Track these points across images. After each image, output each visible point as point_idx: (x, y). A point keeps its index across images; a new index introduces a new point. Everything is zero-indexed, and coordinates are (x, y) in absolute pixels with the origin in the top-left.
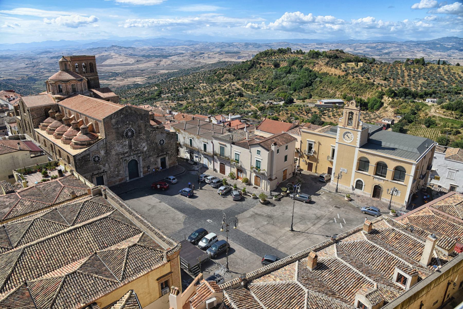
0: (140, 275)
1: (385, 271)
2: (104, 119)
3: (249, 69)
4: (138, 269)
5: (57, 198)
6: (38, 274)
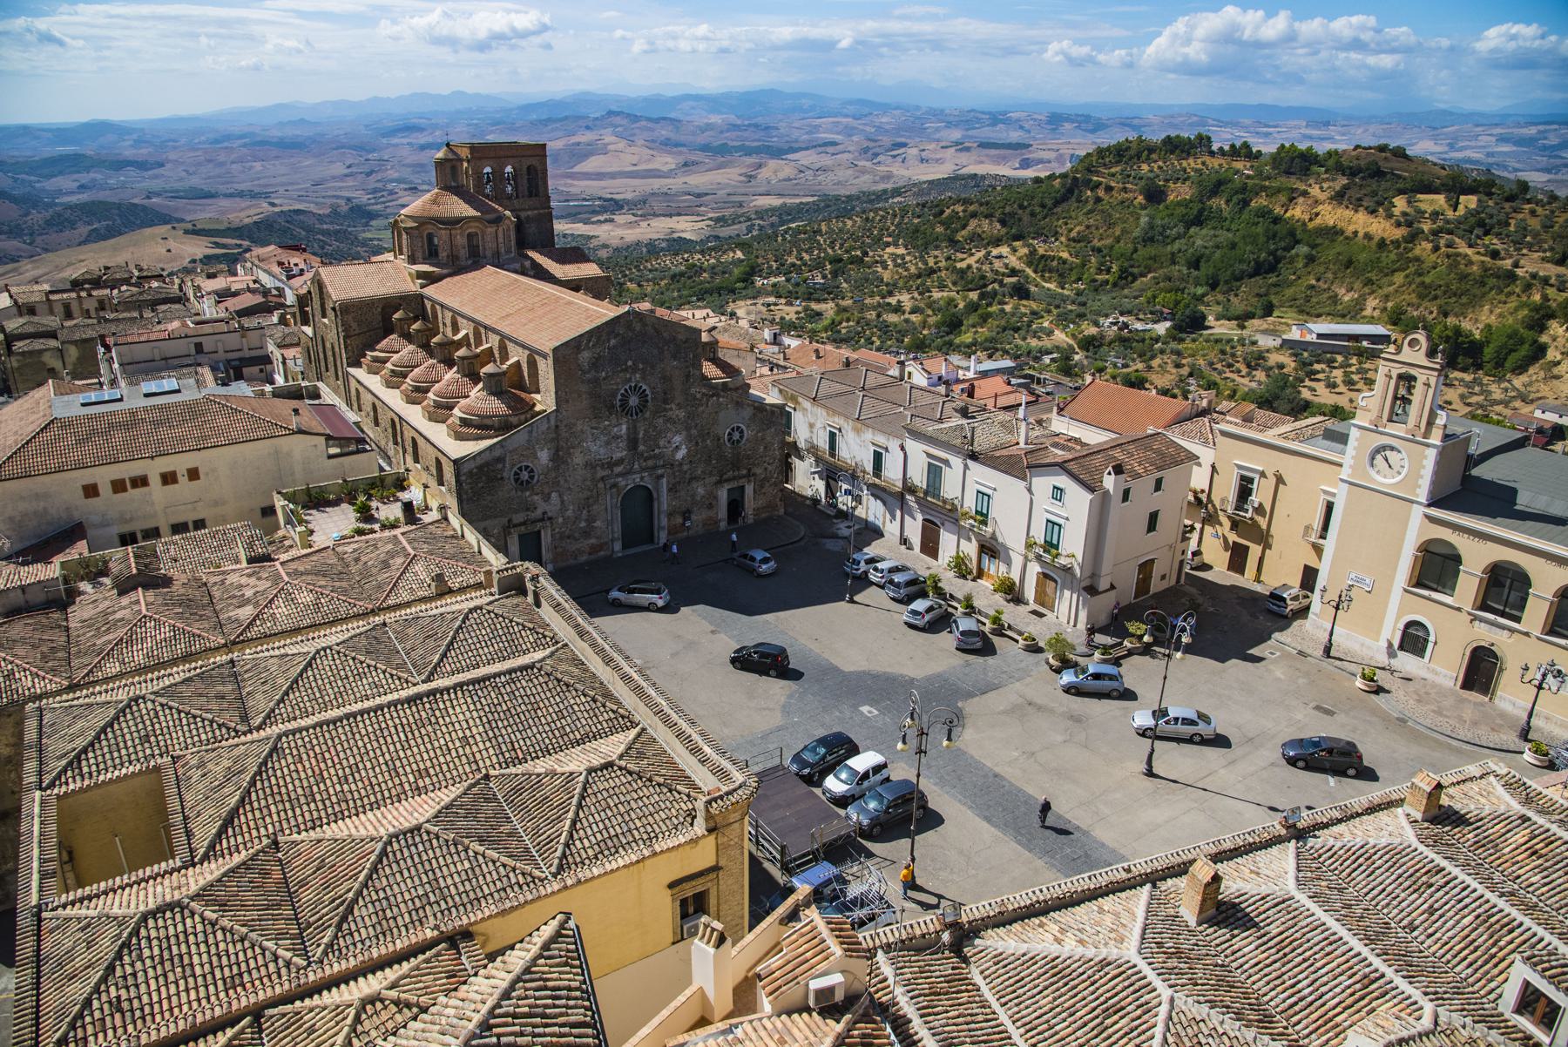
0: (614, 865)
1: (1474, 966)
2: (555, 350)
3: (1057, 203)
4: (610, 843)
5: (392, 589)
6: (313, 821)
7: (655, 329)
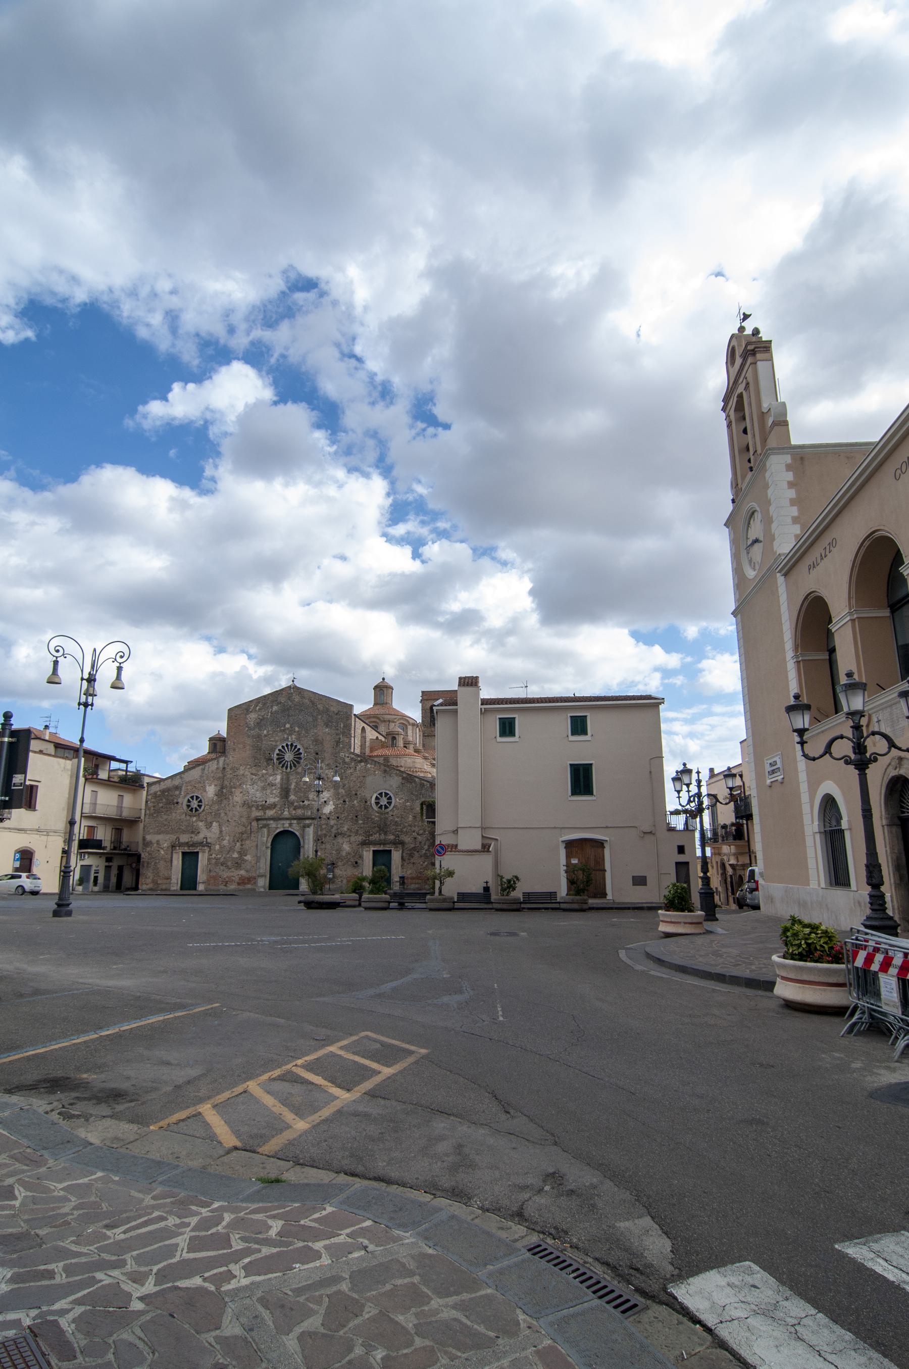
7: (311, 701)
